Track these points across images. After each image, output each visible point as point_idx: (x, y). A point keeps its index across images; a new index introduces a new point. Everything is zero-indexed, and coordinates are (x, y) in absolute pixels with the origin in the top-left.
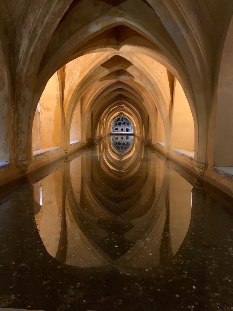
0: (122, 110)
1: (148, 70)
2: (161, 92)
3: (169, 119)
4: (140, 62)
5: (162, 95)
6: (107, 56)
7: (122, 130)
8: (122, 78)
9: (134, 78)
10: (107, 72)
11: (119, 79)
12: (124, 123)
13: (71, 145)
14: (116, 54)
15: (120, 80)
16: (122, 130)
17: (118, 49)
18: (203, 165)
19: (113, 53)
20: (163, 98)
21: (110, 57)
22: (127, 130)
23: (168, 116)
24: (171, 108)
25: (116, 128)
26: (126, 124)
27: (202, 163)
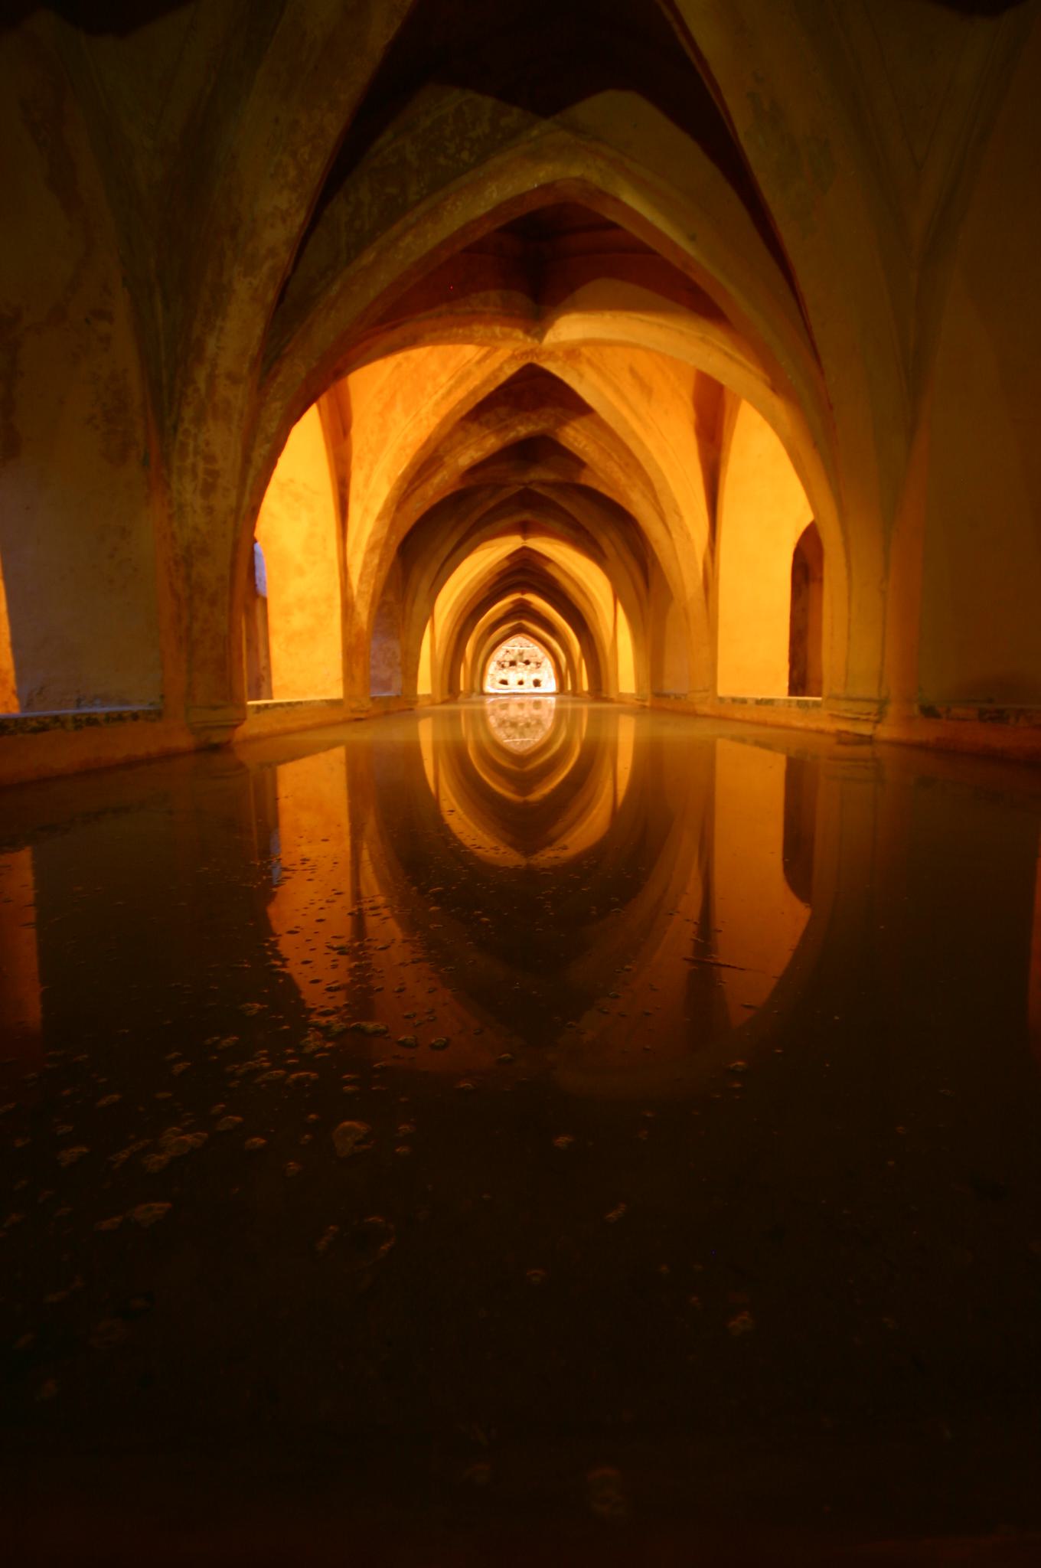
0: (521, 618)
1: (635, 425)
2: (677, 506)
3: (702, 597)
4: (609, 394)
5: (678, 514)
6: (500, 369)
7: (521, 683)
8: (539, 475)
9: (582, 464)
10: (492, 443)
11: (526, 479)
12: (527, 663)
13: (373, 699)
14: (529, 360)
15: (531, 482)
16: (521, 683)
17: (540, 336)
18: (873, 708)
19: (526, 354)
20: (683, 527)
21: (510, 370)
22: (537, 683)
23: (702, 591)
24: (709, 558)
25: (504, 677)
26: (532, 665)
27: (870, 700)
